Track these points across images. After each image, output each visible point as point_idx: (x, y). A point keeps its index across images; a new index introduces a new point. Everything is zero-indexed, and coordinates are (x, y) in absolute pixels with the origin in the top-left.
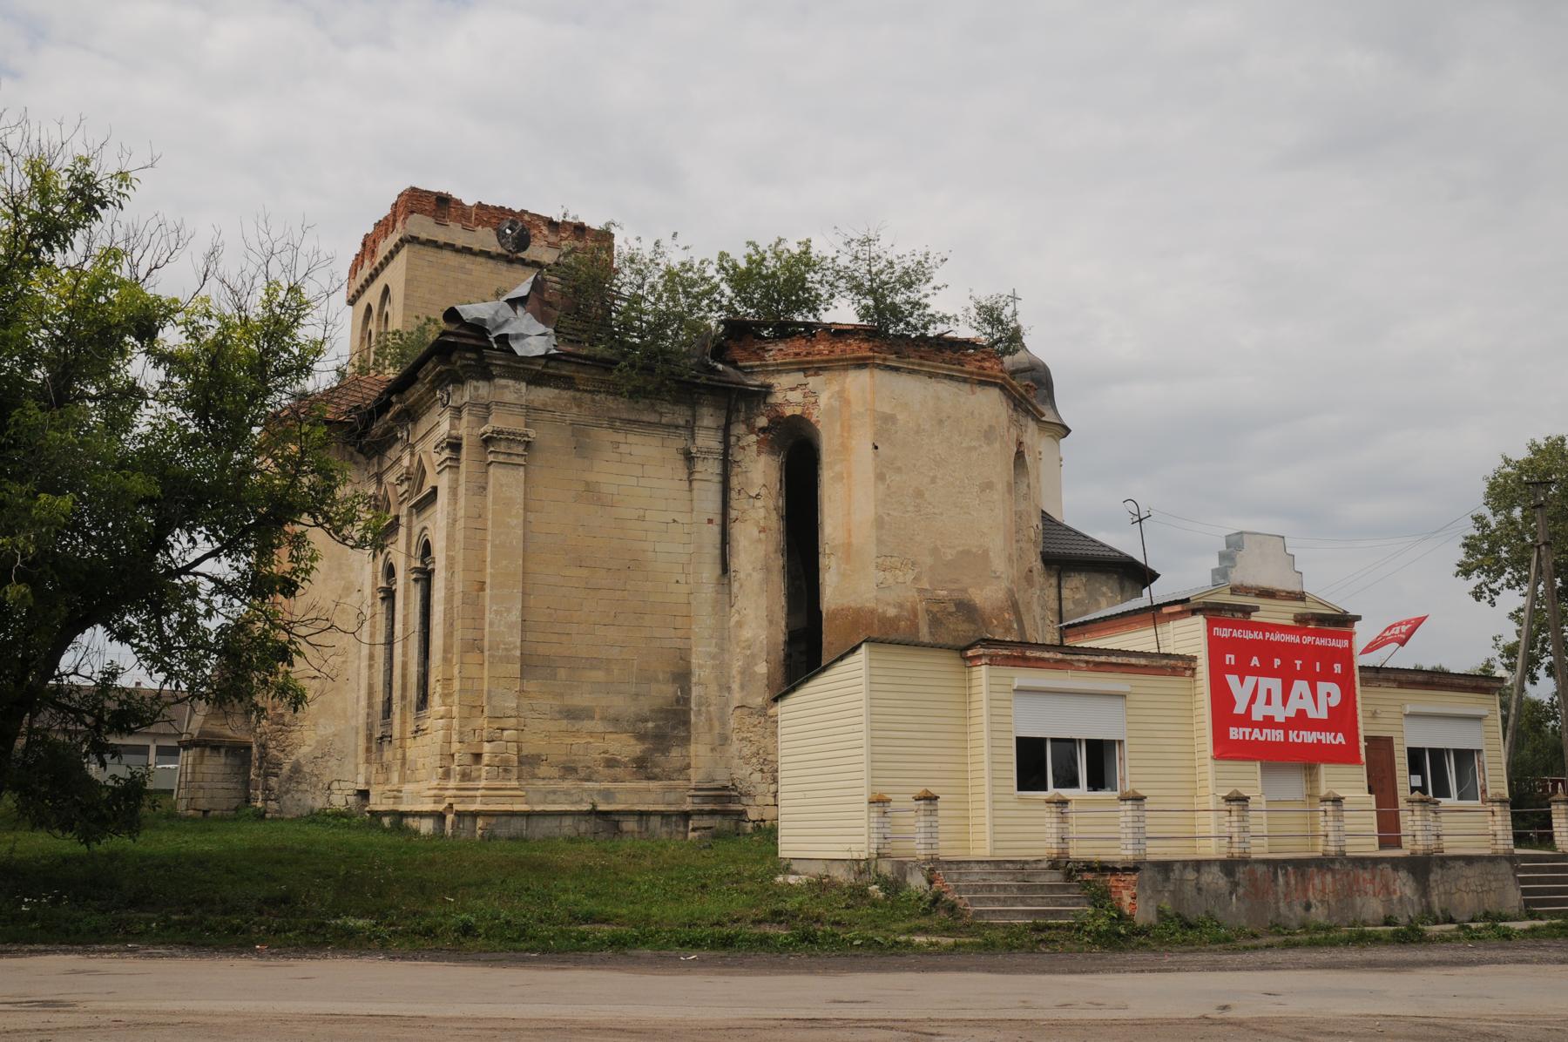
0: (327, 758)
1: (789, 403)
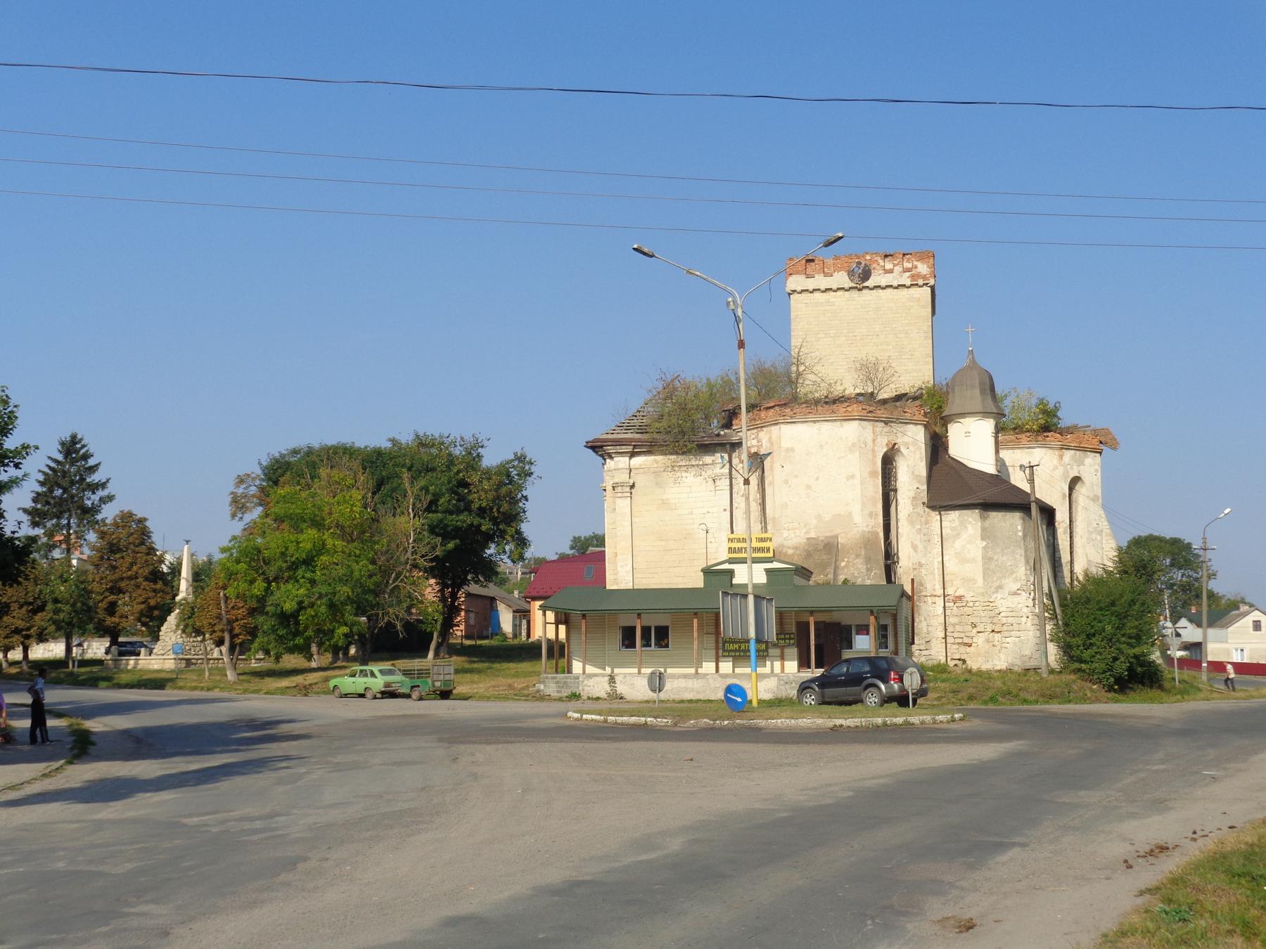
1: (753, 446)
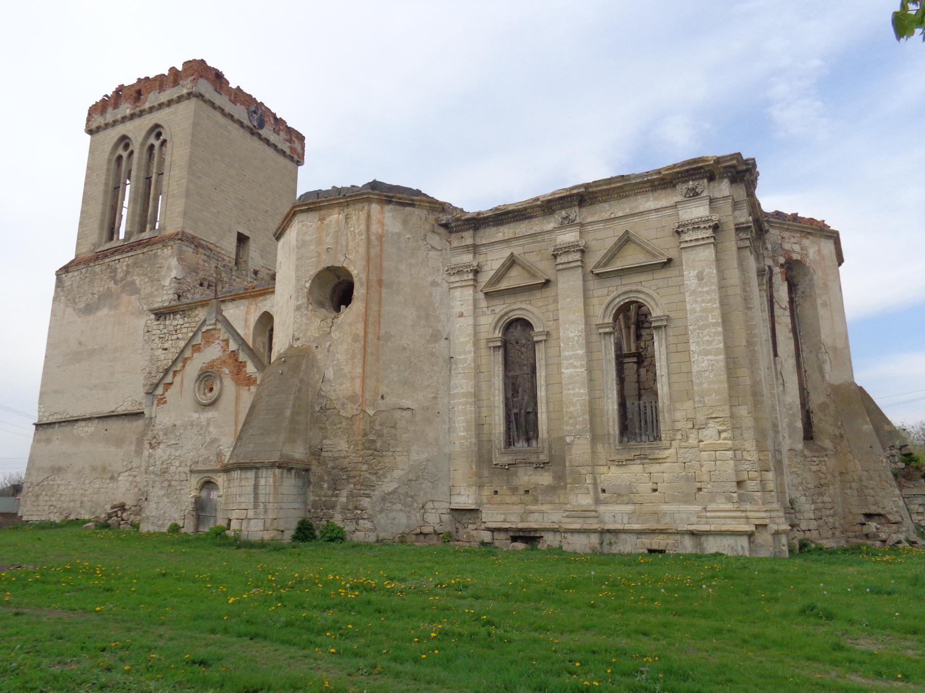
0: (420, 480)
